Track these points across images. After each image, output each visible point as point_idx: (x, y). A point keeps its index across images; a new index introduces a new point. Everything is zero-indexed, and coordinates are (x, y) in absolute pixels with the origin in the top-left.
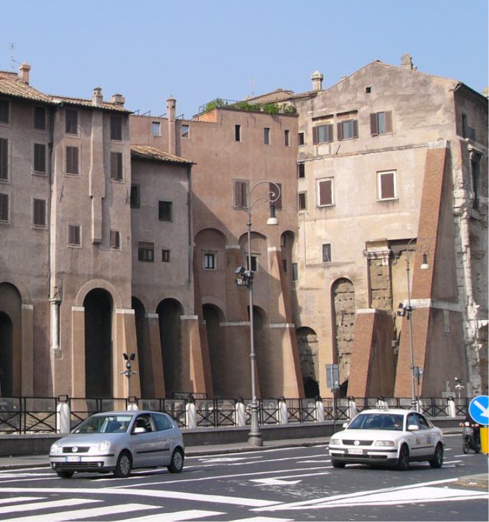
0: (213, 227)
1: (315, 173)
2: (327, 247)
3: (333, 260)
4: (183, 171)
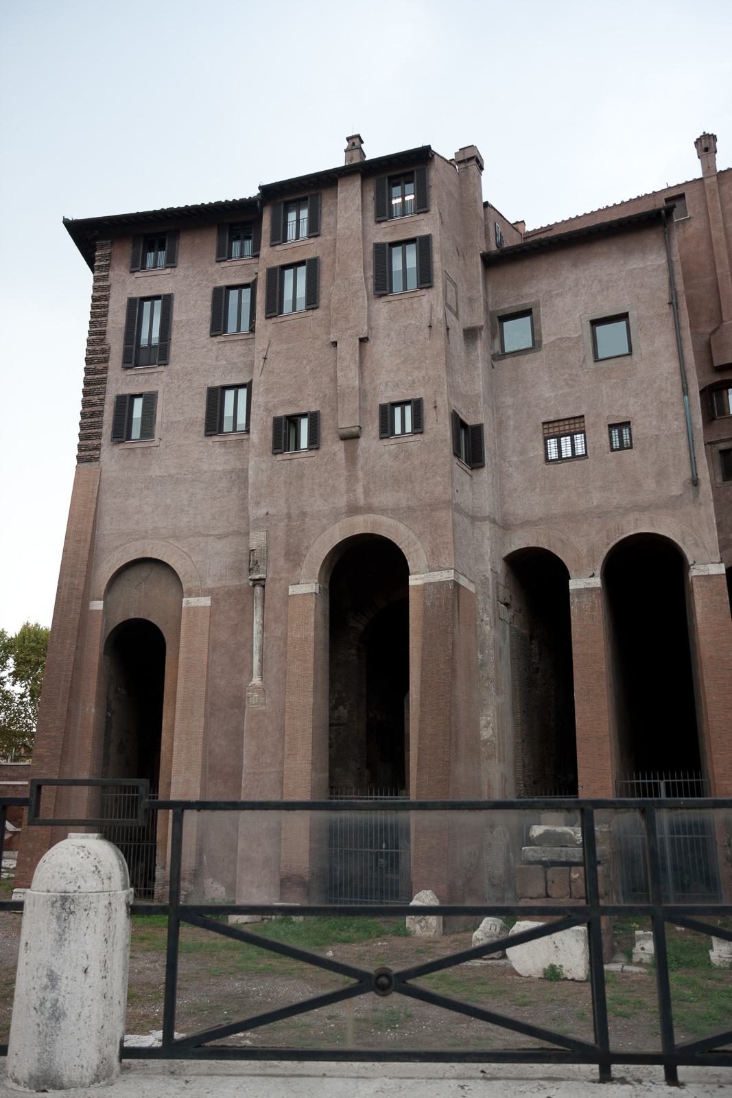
4: (652, 238)
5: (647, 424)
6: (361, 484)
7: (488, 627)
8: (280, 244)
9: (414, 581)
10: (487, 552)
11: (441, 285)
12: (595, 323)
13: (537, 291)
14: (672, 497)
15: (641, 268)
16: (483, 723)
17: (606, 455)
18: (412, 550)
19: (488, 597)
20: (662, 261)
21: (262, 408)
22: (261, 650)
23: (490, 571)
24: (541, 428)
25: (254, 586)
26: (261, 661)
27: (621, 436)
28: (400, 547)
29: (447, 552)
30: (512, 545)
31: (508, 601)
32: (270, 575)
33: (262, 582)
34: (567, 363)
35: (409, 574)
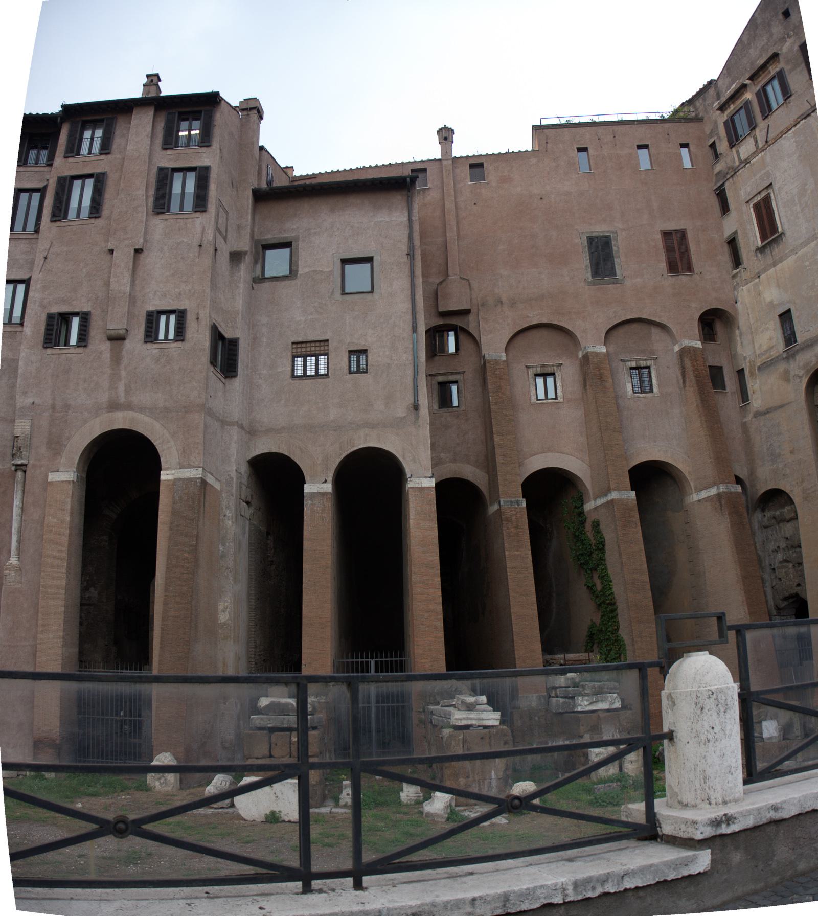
0: (545, 321)
1: (742, 193)
2: (786, 317)
3: (800, 338)
4: (398, 199)
5: (381, 353)
6: (123, 382)
7: (230, 522)
8: (73, 157)
9: (165, 476)
10: (234, 454)
11: (214, 210)
12: (345, 261)
13: (298, 228)
14: (397, 418)
15: (387, 222)
16: (221, 607)
17: (345, 377)
18: (165, 447)
19: (232, 495)
20: (404, 219)
21: (37, 304)
22: (20, 532)
23: (234, 471)
24: (290, 347)
25: (16, 470)
26: (19, 542)
27: (358, 362)
28: (155, 444)
29: (197, 452)
30: (257, 450)
31: (249, 499)
32: (31, 462)
33: (24, 468)
34: (318, 293)
35: (160, 469)
